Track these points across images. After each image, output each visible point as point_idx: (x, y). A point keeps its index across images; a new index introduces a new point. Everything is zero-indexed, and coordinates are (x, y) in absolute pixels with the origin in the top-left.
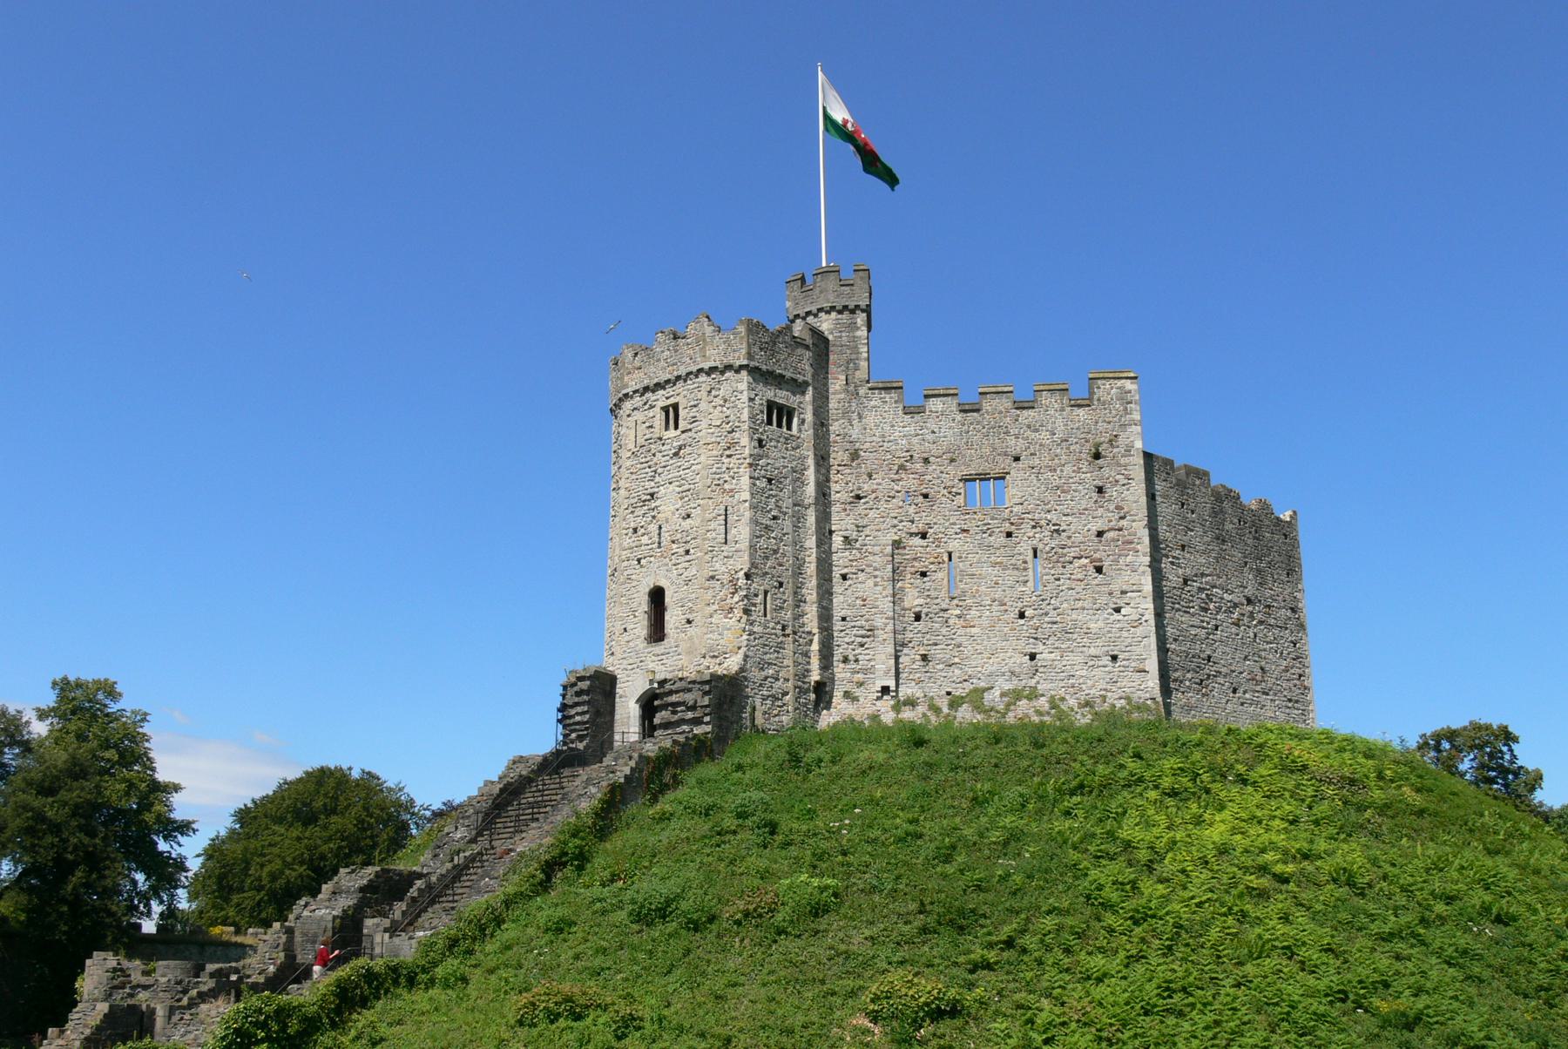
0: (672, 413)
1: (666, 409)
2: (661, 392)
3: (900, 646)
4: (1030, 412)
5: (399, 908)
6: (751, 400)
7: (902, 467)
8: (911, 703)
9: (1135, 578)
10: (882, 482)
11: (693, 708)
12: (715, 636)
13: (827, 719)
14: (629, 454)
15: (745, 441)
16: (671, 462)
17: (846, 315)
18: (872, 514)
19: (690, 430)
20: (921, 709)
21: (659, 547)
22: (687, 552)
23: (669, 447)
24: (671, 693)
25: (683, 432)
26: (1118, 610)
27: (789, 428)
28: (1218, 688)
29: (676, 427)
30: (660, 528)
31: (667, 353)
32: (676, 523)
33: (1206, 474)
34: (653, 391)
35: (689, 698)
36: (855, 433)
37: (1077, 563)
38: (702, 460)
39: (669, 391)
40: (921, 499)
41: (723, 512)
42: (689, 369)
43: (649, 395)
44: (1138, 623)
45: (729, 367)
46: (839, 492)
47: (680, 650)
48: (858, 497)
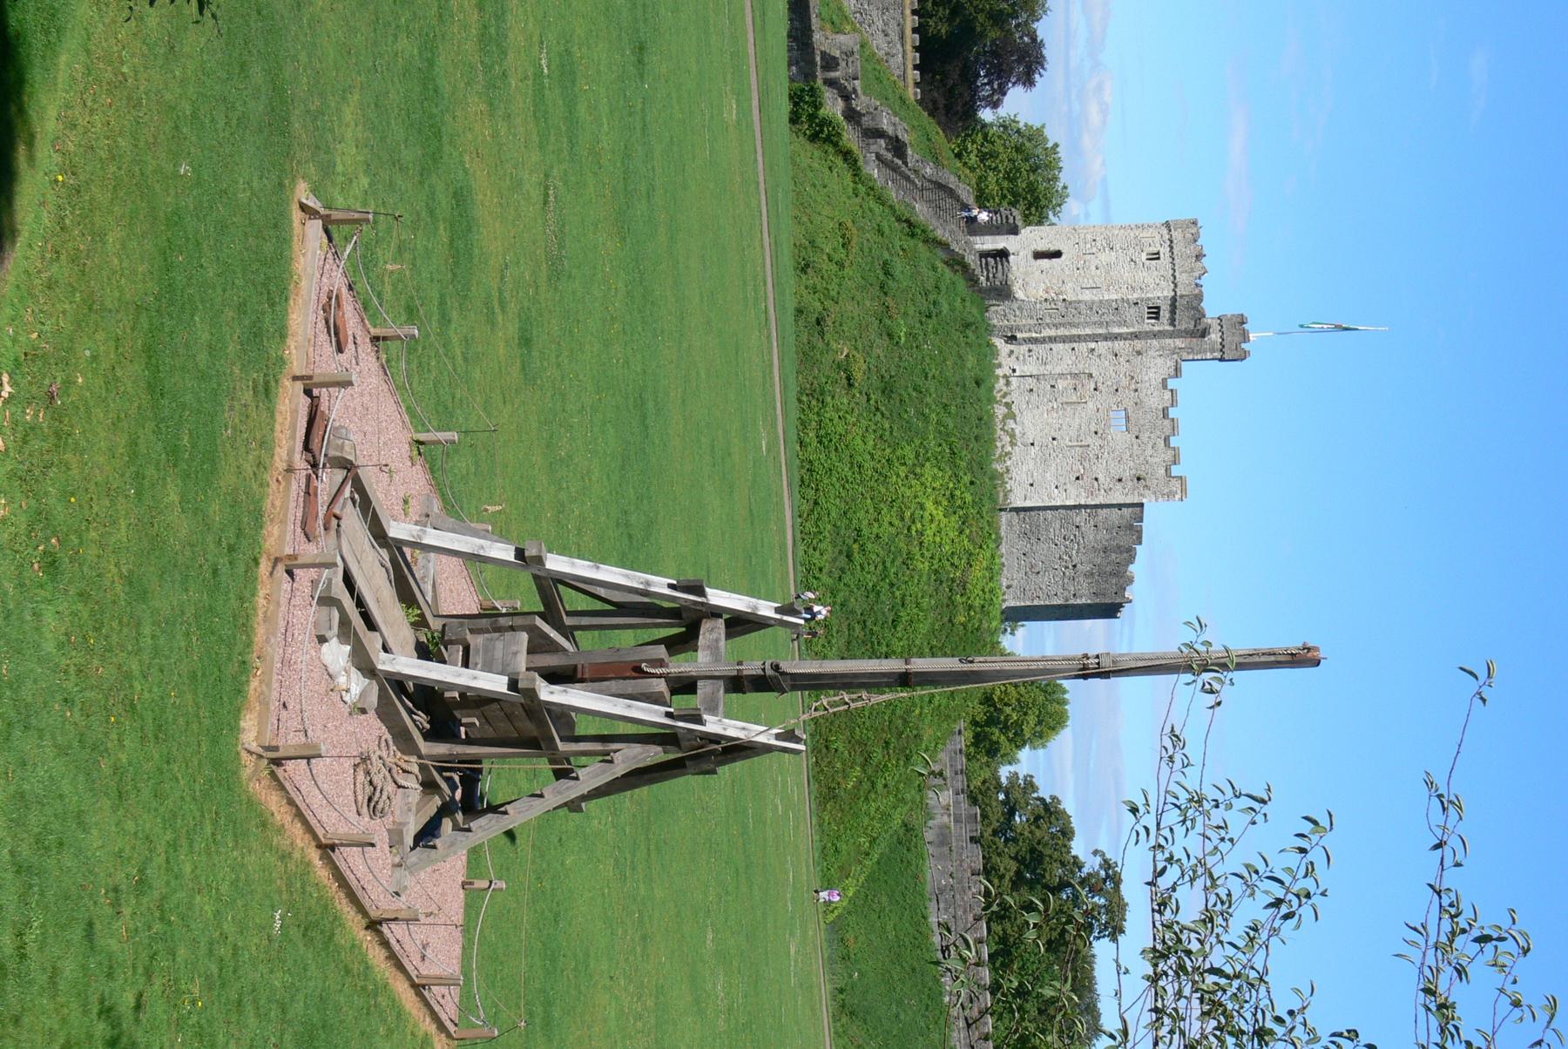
1: (1158, 253)
3: (1038, 377)
5: (889, 156)
6: (1159, 298)
7: (1132, 378)
8: (1008, 384)
9: (1073, 496)
10: (1124, 367)
11: (994, 277)
13: (999, 342)
15: (1135, 296)
18: (1107, 363)
20: (1005, 388)
24: (1002, 265)
26: (1057, 487)
27: (1149, 318)
28: (1022, 544)
29: (1148, 259)
32: (1093, 262)
33: (1140, 543)
35: (999, 274)
36: (1151, 353)
37: (1081, 467)
38: (1125, 273)
39: (1168, 254)
43: (1168, 243)
44: (1050, 497)
45: (1176, 286)
46: (1118, 345)
48: (1116, 355)
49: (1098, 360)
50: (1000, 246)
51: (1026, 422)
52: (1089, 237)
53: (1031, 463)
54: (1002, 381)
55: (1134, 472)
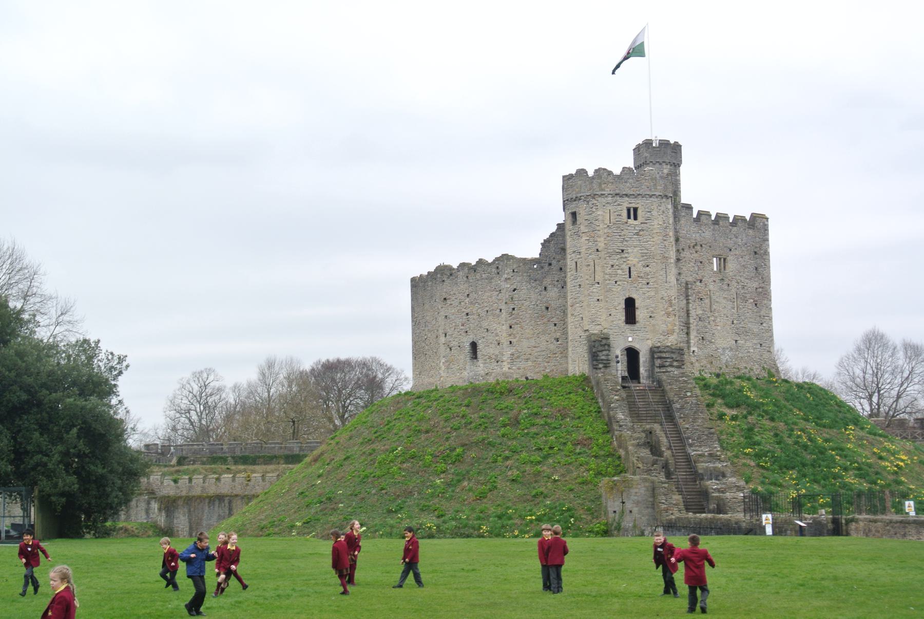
0: (633, 213)
2: (627, 199)
11: (677, 361)
14: (606, 226)
16: (635, 236)
19: (646, 223)
21: (630, 277)
22: (648, 284)
23: (633, 228)
25: (642, 223)
29: (635, 218)
30: (630, 268)
31: (631, 181)
34: (620, 197)
35: (674, 356)
40: (699, 264)
41: (664, 267)
47: (646, 330)
50: (618, 352)
52: (608, 271)
53: (749, 344)
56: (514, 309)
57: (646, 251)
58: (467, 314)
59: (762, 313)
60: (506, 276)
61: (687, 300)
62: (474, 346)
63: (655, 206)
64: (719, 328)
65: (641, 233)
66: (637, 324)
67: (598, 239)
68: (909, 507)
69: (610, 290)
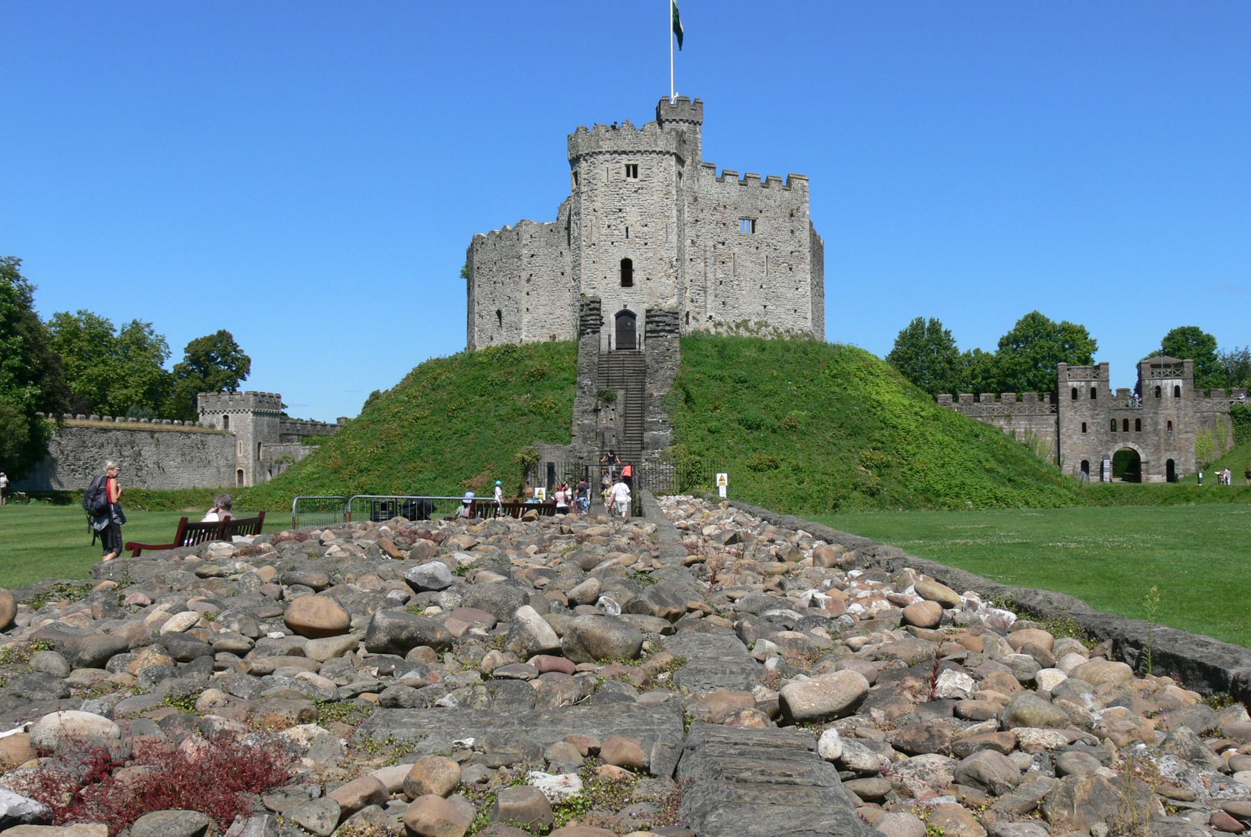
0: (633, 170)
2: (625, 156)
4: (767, 190)
8: (720, 324)
10: (706, 215)
11: (669, 325)
12: (663, 288)
15: (674, 192)
17: (692, 125)
18: (703, 230)
20: (725, 328)
21: (627, 237)
22: (646, 244)
24: (655, 316)
29: (635, 176)
30: (627, 228)
34: (619, 154)
36: (696, 188)
39: (631, 156)
40: (722, 225)
42: (646, 149)
44: (804, 296)
48: (697, 221)
49: (700, 239)
51: (749, 311)
52: (604, 231)
54: (720, 330)
55: (787, 219)
56: (531, 275)
57: (644, 210)
58: (495, 283)
59: (800, 276)
60: (524, 242)
61: (705, 262)
62: (499, 313)
63: (655, 163)
64: (743, 292)
65: (640, 191)
66: (634, 287)
67: (595, 199)
68: (721, 480)
69: (606, 251)
